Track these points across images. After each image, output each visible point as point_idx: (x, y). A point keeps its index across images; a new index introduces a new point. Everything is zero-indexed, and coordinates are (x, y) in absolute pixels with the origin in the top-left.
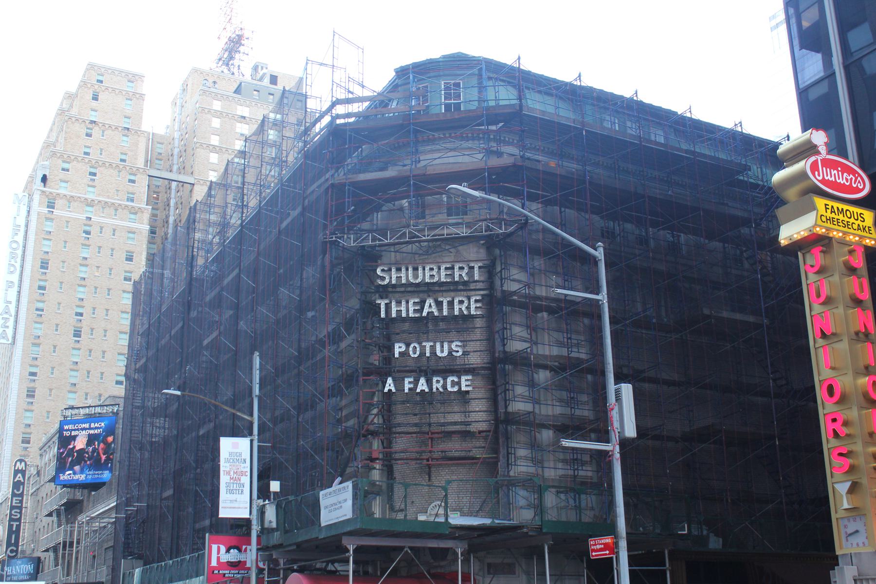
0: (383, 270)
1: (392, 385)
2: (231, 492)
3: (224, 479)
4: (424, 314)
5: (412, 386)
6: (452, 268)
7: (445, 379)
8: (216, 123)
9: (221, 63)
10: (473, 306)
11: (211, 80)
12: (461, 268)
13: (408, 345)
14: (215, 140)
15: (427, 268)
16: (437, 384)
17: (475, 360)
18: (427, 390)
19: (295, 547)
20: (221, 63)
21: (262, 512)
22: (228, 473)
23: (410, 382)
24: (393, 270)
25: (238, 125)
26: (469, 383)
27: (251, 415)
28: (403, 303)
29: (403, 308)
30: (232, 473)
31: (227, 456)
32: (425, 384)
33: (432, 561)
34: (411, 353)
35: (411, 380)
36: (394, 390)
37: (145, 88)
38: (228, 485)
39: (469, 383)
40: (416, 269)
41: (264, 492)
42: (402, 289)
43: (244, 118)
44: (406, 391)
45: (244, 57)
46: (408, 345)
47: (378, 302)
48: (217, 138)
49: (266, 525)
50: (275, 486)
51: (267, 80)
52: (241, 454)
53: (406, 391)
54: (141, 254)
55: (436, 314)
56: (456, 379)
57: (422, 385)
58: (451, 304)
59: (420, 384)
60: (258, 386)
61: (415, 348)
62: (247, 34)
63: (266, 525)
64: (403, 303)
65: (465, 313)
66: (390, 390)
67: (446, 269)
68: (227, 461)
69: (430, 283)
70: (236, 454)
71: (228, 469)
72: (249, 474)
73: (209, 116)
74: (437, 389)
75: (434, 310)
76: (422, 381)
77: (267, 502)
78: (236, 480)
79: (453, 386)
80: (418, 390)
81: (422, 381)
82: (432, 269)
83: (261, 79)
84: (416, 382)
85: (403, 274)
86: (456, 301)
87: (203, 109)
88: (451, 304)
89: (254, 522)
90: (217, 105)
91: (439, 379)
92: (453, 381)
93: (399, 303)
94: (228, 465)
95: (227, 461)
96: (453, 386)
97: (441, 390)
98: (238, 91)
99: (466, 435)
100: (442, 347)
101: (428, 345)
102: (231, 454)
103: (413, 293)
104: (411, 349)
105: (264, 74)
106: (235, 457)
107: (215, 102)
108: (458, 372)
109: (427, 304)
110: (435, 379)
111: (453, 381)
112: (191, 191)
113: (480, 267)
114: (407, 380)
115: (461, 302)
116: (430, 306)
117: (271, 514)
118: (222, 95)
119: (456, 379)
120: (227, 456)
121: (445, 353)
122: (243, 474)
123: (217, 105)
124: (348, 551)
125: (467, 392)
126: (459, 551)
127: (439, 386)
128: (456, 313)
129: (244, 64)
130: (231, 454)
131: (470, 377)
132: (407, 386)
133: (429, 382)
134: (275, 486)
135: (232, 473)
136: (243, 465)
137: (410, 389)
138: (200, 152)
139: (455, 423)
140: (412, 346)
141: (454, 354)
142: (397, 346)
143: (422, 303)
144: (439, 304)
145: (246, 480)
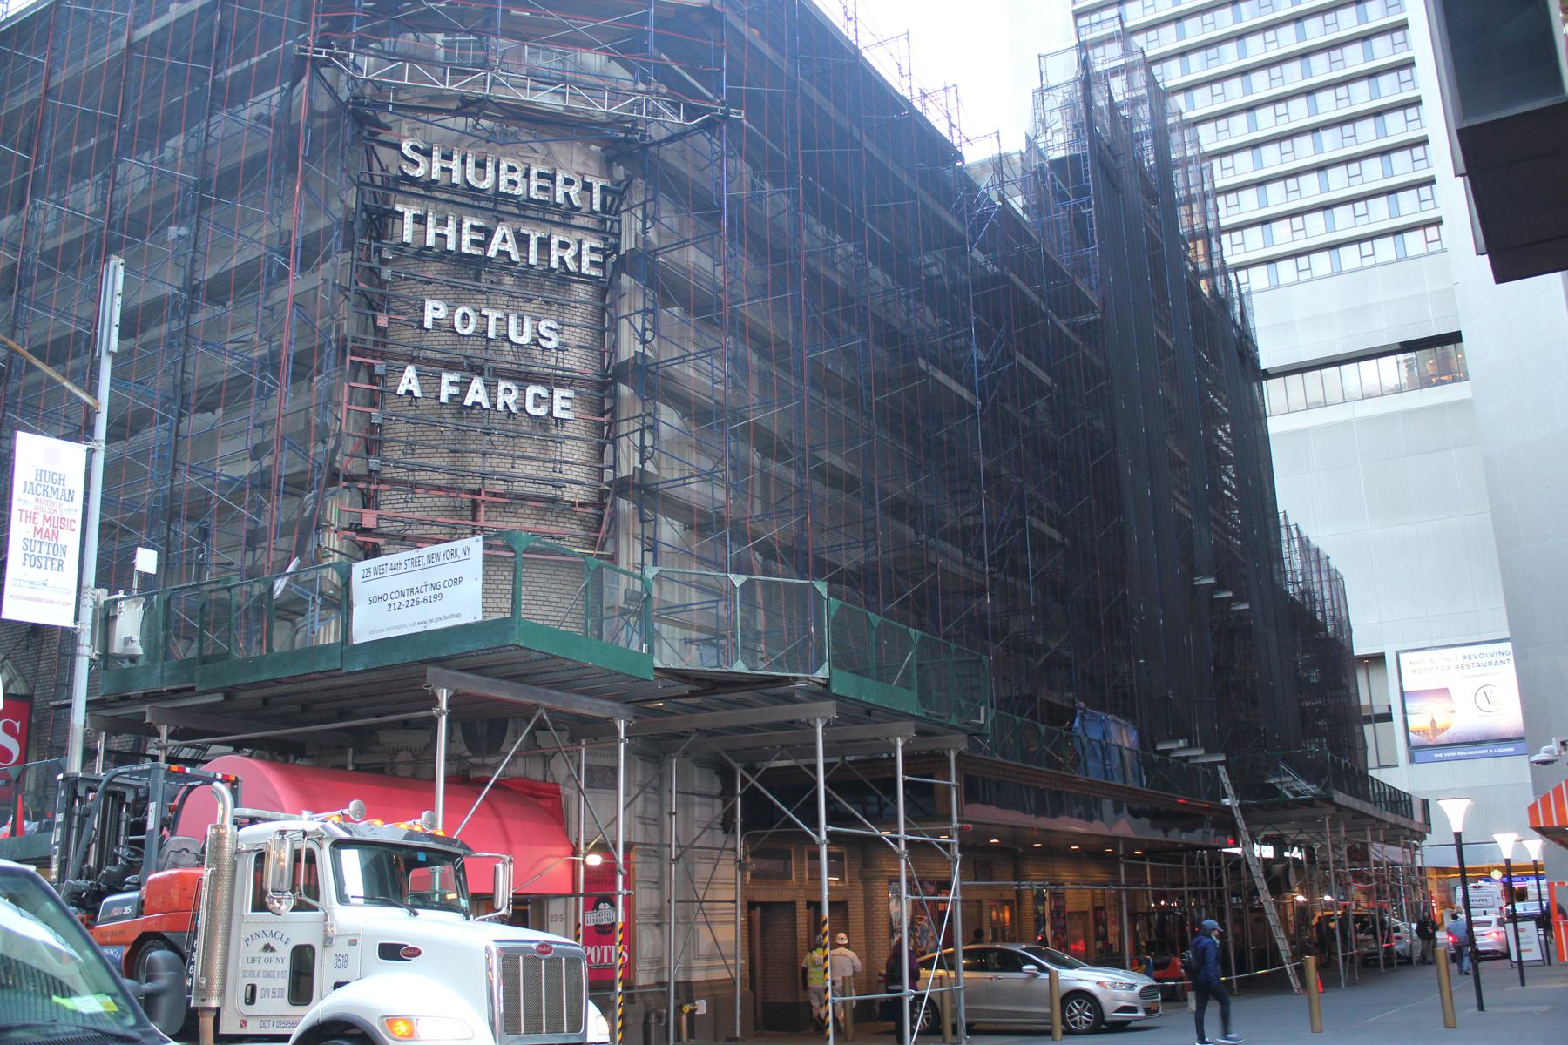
0: (414, 148)
1: (415, 382)
2: (34, 561)
3: (19, 531)
4: (492, 253)
5: (455, 390)
6: (552, 178)
7: (522, 390)
10: (585, 259)
12: (569, 182)
13: (452, 308)
15: (503, 166)
16: (507, 395)
17: (574, 362)
18: (486, 405)
19: (219, 698)
21: (106, 619)
22: (31, 517)
23: (452, 383)
24: (436, 154)
26: (567, 404)
27: (93, 390)
28: (452, 224)
29: (450, 231)
30: (39, 519)
31: (31, 478)
32: (483, 391)
33: (468, 753)
34: (458, 325)
35: (455, 377)
36: (417, 393)
38: (27, 545)
39: (567, 404)
40: (481, 165)
41: (113, 570)
44: (444, 399)
46: (452, 308)
47: (399, 208)
49: (117, 648)
50: (146, 560)
52: (63, 479)
53: (444, 399)
55: (515, 257)
56: (544, 393)
57: (476, 393)
58: (544, 244)
59: (472, 390)
60: (116, 331)
61: (465, 316)
63: (117, 648)
64: (452, 224)
65: (572, 267)
66: (409, 393)
67: (541, 175)
68: (30, 488)
69: (506, 195)
70: (55, 473)
71: (30, 508)
72: (78, 526)
74: (506, 406)
75: (511, 247)
76: (477, 384)
77: (121, 595)
78: (47, 535)
79: (536, 406)
80: (468, 402)
81: (477, 384)
82: (512, 170)
84: (464, 386)
85: (455, 165)
86: (555, 242)
88: (544, 244)
89: (85, 638)
91: (510, 385)
92: (537, 395)
94: (31, 498)
95: (30, 488)
96: (536, 406)
97: (514, 409)
99: (552, 505)
100: (520, 325)
101: (493, 315)
102: (39, 473)
103: (474, 209)
104: (458, 317)
106: (49, 483)
108: (552, 380)
109: (498, 236)
110: (502, 385)
111: (537, 395)
113: (603, 188)
114: (447, 378)
116: (504, 240)
117: (130, 622)
119: (544, 393)
120: (31, 478)
121: (525, 339)
122: (63, 523)
124: (435, 701)
125: (560, 422)
126: (621, 725)
127: (511, 400)
128: (554, 264)
130: (39, 473)
131: (569, 393)
132: (446, 391)
133: (491, 388)
134: (146, 560)
135: (39, 519)
136: (66, 505)
137: (451, 396)
139: (534, 480)
140: (460, 311)
141: (543, 342)
142: (430, 305)
143: (489, 234)
144: (522, 241)
145: (71, 539)
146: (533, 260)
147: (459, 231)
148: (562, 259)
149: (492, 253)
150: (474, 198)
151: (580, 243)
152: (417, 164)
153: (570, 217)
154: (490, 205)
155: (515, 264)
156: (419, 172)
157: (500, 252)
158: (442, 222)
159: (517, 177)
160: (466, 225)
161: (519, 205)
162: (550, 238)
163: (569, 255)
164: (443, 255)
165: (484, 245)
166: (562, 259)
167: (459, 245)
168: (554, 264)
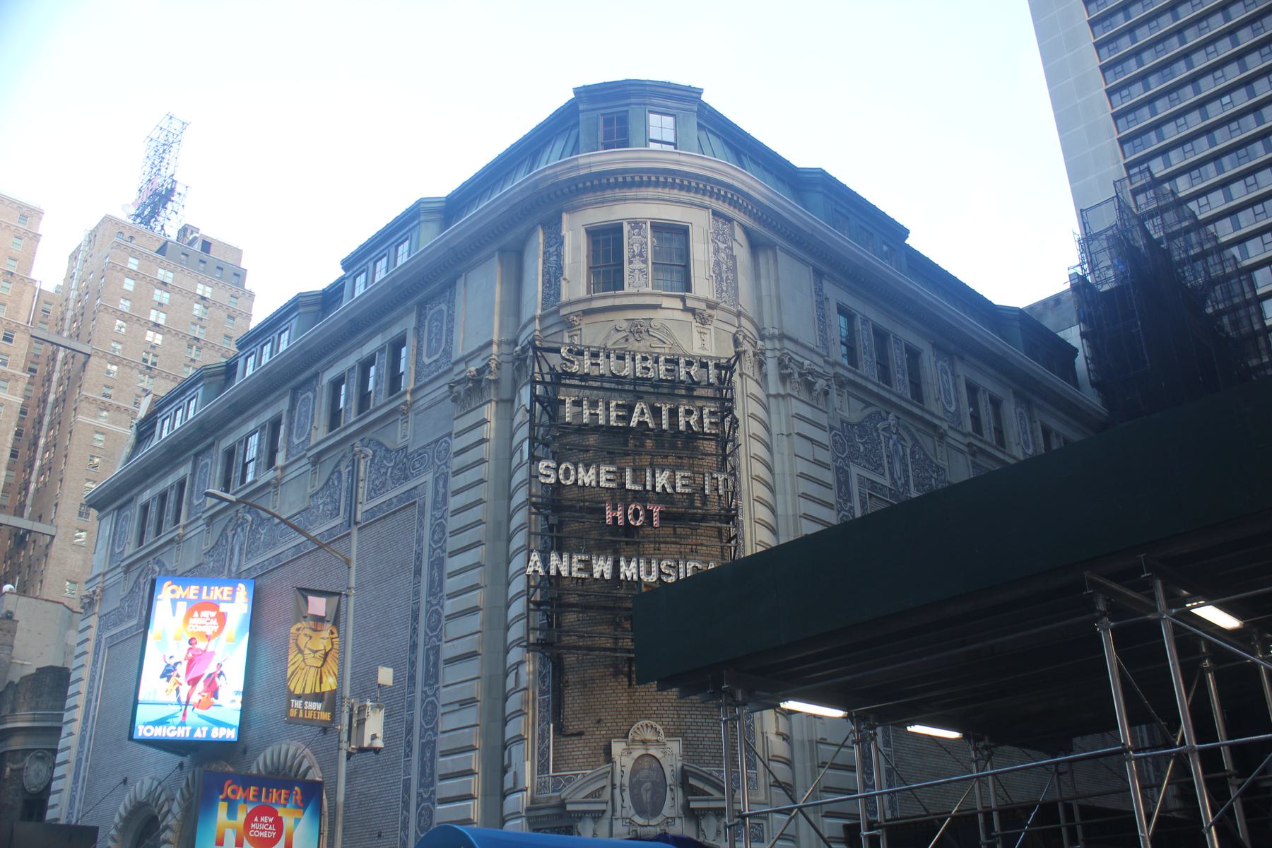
4: (633, 423)
8: (129, 285)
9: (138, 220)
10: (706, 421)
11: (127, 235)
14: (125, 305)
20: (138, 220)
25: (157, 292)
37: (45, 228)
42: (598, 384)
43: (165, 284)
45: (173, 216)
48: (128, 303)
51: (197, 247)
54: (7, 433)
58: (673, 413)
62: (179, 188)
69: (642, 379)
73: (120, 275)
75: (647, 418)
83: (191, 243)
86: (681, 409)
87: (115, 266)
88: (673, 413)
90: (133, 264)
93: (594, 404)
98: (162, 250)
105: (195, 238)
107: (131, 260)
109: (637, 410)
112: (85, 364)
115: (689, 413)
116: (642, 413)
118: (141, 253)
123: (133, 264)
128: (682, 428)
129: (169, 224)
138: (104, 318)
143: (631, 409)
144: (656, 412)
146: (665, 427)
147: (607, 409)
148: (688, 423)
149: (633, 423)
150: (618, 383)
151: (701, 409)
152: (572, 362)
153: (693, 390)
154: (631, 388)
155: (652, 430)
156: (575, 368)
157: (639, 422)
158: (594, 404)
159: (649, 364)
160: (613, 404)
161: (653, 386)
162: (677, 408)
163: (693, 420)
164: (596, 429)
165: (628, 418)
166: (688, 423)
167: (608, 420)
168: (682, 428)
